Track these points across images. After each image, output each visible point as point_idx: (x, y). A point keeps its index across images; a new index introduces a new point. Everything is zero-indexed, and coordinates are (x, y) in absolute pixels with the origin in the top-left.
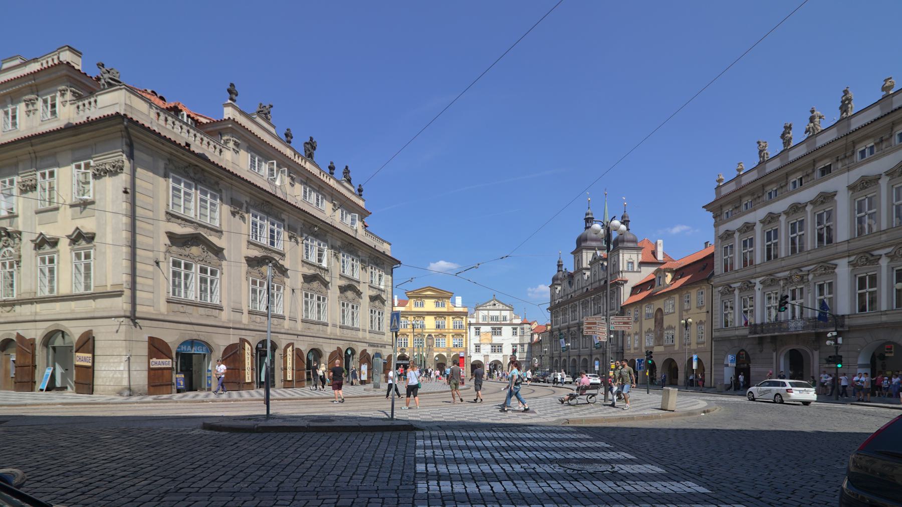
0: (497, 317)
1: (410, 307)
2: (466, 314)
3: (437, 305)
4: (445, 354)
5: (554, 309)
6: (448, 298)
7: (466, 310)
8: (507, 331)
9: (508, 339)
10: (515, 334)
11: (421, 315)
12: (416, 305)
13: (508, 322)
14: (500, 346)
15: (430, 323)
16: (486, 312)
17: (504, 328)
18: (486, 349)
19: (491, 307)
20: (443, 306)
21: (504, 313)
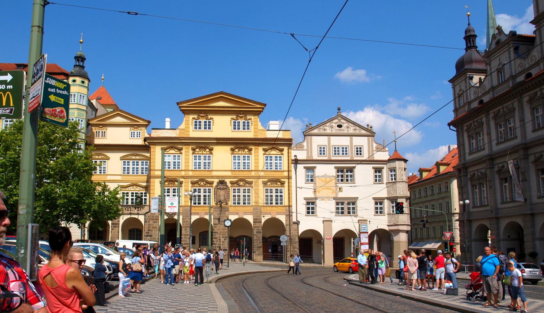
0: (345, 150)
1: (187, 129)
2: (288, 143)
4: (250, 218)
5: (465, 123)
6: (257, 113)
7: (287, 136)
8: (364, 173)
9: (365, 187)
10: (378, 180)
11: (204, 145)
12: (197, 126)
13: (365, 157)
14: (353, 202)
15: (222, 160)
16: (323, 141)
17: (359, 170)
18: (326, 208)
19: (336, 130)
20: (246, 127)
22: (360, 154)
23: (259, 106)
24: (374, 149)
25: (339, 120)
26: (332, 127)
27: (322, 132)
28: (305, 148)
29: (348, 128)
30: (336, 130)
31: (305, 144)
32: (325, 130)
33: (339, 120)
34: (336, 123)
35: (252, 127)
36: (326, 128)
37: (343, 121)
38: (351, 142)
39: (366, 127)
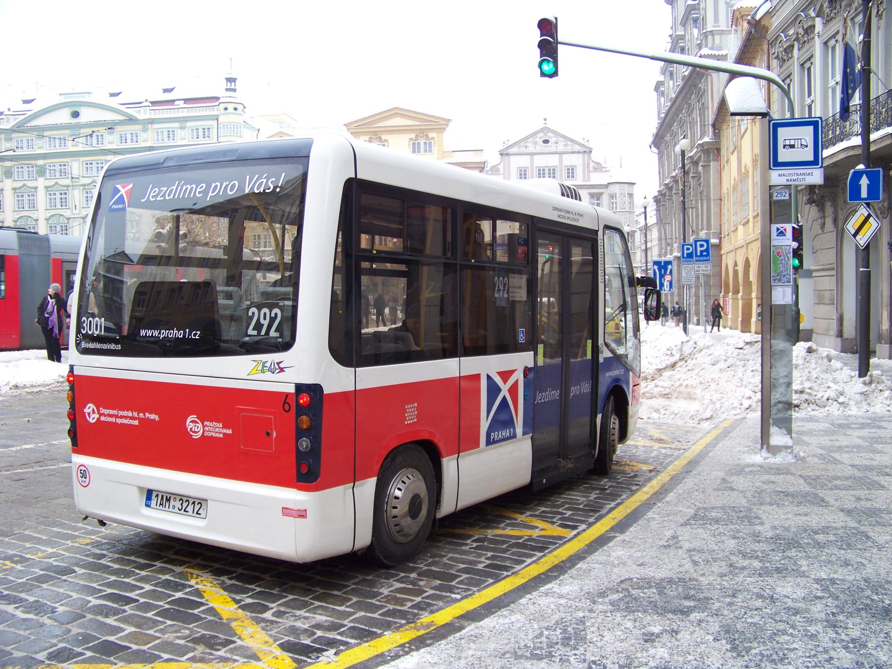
3: (416, 149)
21: (569, 160)
22: (573, 177)
23: (442, 122)
24: (591, 169)
25: (546, 134)
26: (536, 143)
27: (523, 150)
28: (502, 171)
29: (557, 143)
30: (541, 147)
31: (501, 167)
32: (526, 147)
33: (546, 134)
34: (541, 138)
35: (435, 149)
36: (528, 144)
37: (550, 134)
38: (561, 161)
39: (582, 142)
